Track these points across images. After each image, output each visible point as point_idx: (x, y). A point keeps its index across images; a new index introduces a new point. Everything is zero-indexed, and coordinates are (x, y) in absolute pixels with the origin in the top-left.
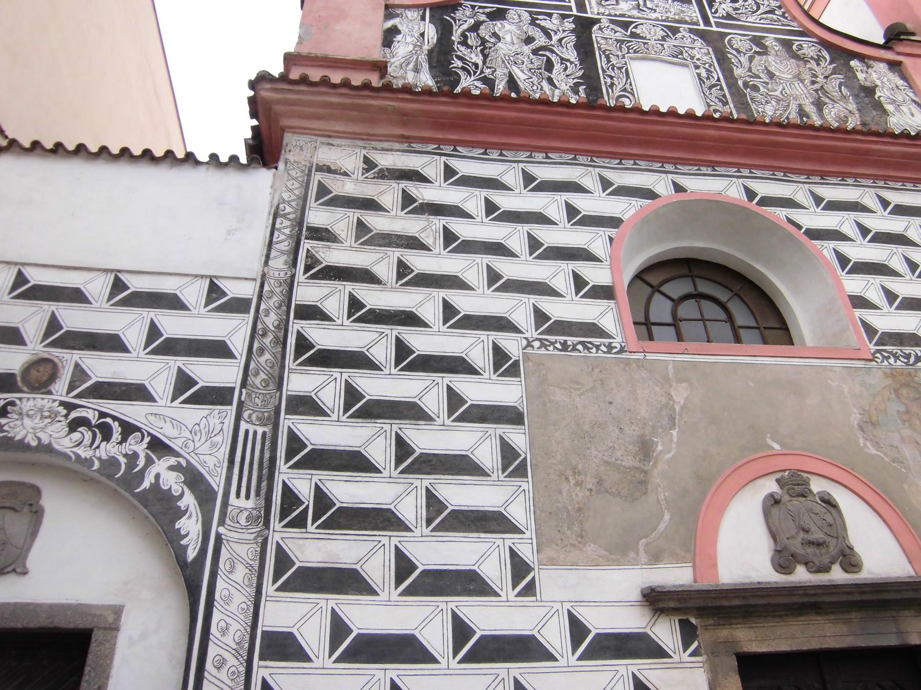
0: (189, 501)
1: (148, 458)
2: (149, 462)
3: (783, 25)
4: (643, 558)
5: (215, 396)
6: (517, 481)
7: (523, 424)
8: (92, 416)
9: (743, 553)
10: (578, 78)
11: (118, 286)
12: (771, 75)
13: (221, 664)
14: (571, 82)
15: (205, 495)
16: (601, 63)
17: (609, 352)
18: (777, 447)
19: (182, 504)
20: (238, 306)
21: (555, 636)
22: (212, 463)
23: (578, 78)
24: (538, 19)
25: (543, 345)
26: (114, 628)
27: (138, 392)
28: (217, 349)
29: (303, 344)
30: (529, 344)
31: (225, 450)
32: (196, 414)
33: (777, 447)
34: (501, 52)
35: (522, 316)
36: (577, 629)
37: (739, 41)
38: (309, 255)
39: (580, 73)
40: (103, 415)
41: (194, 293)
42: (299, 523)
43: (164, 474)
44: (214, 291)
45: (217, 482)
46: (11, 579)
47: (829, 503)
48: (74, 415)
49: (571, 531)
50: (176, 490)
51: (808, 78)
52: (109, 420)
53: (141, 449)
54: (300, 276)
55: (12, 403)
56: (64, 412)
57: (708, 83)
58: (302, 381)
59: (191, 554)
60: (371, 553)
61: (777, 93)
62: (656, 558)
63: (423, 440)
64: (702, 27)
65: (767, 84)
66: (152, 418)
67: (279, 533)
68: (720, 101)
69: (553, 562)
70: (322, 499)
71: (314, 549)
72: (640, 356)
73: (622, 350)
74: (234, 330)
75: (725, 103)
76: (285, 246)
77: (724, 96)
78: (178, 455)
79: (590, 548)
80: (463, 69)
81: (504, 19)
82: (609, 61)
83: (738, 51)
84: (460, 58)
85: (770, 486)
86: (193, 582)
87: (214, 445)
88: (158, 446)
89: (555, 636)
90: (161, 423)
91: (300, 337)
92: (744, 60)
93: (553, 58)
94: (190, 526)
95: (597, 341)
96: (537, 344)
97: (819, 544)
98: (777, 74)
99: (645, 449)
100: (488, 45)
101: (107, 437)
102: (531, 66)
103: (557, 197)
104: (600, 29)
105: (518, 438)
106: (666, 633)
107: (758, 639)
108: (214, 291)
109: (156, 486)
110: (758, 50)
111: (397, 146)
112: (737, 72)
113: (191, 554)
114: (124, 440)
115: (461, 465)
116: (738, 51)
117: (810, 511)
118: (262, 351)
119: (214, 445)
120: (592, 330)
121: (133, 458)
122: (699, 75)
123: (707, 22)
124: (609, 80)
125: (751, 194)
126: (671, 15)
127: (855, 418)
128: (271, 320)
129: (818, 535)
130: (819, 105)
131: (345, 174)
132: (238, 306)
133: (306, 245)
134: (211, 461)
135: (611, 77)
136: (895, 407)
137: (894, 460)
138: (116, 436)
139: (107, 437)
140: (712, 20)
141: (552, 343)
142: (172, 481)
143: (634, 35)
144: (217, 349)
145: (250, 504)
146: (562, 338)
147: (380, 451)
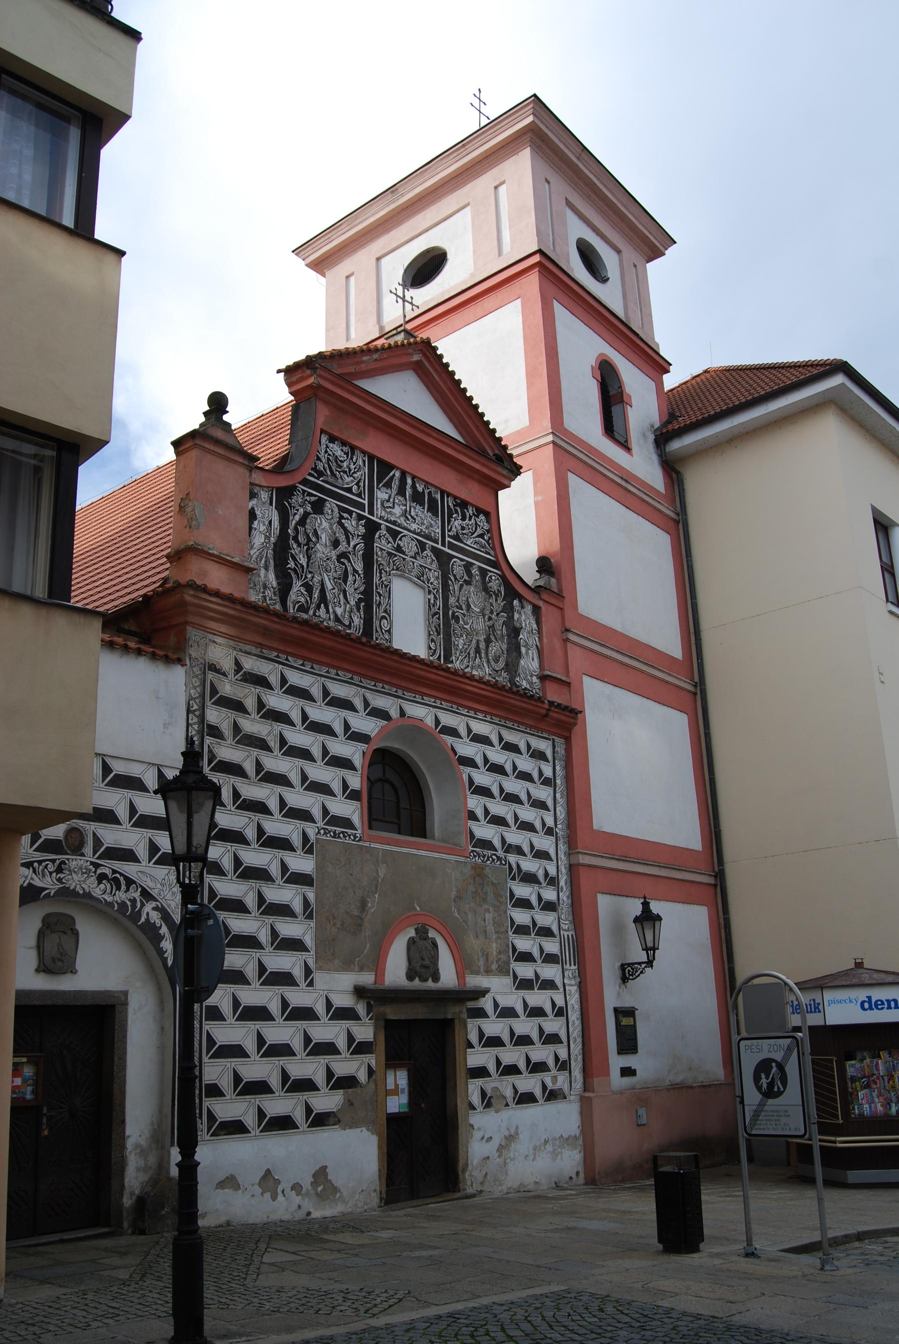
0: (164, 930)
1: (141, 901)
2: (143, 905)
6: (309, 922)
7: (313, 886)
8: (108, 871)
12: (469, 607)
16: (376, 580)
17: (354, 840)
18: (418, 909)
19: (161, 932)
21: (320, 1008)
23: (361, 593)
25: (325, 833)
27: (129, 855)
30: (319, 833)
33: (418, 909)
34: (319, 555)
36: (329, 1005)
39: (362, 589)
40: (114, 872)
46: (69, 976)
47: (435, 945)
48: (99, 871)
49: (331, 954)
50: (158, 922)
52: (117, 875)
53: (137, 895)
55: (63, 863)
56: (93, 869)
60: (248, 962)
61: (467, 627)
62: (361, 969)
64: (439, 546)
66: (140, 874)
68: (437, 630)
72: (367, 844)
75: (439, 634)
77: (439, 625)
78: (156, 900)
80: (294, 570)
81: (322, 513)
84: (294, 559)
87: (173, 893)
88: (146, 895)
89: (320, 1008)
90: (144, 879)
95: (350, 831)
96: (322, 832)
101: (119, 888)
103: (340, 713)
104: (380, 537)
106: (361, 1009)
109: (147, 920)
110: (467, 578)
111: (254, 650)
112: (452, 600)
114: (127, 890)
115: (284, 910)
116: (455, 576)
117: (426, 948)
119: (173, 893)
120: (346, 823)
121: (133, 901)
122: (429, 600)
124: (378, 598)
125: (437, 722)
126: (423, 528)
129: (427, 962)
130: (488, 641)
131: (224, 674)
134: (173, 904)
135: (380, 595)
136: (471, 888)
137: (464, 921)
138: (123, 887)
139: (119, 888)
141: (330, 832)
142: (155, 917)
143: (399, 549)
147: (250, 901)
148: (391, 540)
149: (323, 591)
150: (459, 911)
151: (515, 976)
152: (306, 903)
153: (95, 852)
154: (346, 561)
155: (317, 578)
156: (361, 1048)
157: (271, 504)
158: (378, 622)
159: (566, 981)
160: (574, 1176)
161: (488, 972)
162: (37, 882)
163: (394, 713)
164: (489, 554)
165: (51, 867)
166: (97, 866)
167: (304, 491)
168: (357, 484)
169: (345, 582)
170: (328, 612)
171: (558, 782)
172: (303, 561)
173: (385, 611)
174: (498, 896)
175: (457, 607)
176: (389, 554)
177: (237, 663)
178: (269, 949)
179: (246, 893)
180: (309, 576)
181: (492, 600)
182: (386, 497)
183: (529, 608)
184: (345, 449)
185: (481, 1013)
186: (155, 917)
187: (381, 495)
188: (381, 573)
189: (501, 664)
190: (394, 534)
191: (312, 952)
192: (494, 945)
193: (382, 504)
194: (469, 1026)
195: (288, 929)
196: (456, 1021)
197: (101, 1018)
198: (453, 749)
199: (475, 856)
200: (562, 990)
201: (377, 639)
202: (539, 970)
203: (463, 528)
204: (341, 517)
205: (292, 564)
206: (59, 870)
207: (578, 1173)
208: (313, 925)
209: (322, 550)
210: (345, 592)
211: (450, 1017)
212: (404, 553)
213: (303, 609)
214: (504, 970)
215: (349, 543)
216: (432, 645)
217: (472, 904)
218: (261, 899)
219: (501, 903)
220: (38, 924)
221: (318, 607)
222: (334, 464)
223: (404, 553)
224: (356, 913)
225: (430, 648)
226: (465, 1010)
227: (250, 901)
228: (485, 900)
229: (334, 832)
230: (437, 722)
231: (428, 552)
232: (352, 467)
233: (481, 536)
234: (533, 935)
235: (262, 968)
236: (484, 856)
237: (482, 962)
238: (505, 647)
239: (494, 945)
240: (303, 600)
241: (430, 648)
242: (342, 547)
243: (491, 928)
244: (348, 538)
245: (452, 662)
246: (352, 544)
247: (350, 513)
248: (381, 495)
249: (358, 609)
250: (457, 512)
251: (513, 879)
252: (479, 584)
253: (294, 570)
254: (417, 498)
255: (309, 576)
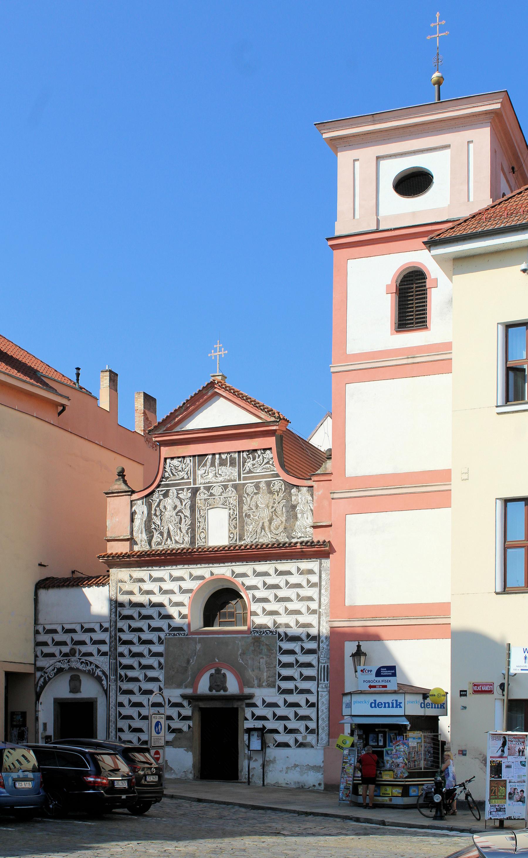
0: (103, 678)
2: (96, 670)
3: (271, 471)
4: (184, 687)
5: (105, 654)
6: (161, 670)
9: (203, 686)
10: (189, 525)
11: (82, 627)
12: (257, 506)
13: (112, 708)
14: (187, 528)
15: (106, 676)
16: (197, 515)
18: (217, 661)
20: (106, 630)
22: (106, 669)
23: (189, 525)
24: (179, 494)
25: (169, 635)
26: (97, 702)
27: (91, 654)
28: (103, 642)
29: (120, 639)
31: (108, 666)
32: (102, 658)
33: (217, 661)
35: (165, 627)
37: (250, 489)
38: (120, 613)
40: (86, 660)
41: (97, 628)
42: (122, 681)
43: (98, 672)
44: (101, 626)
45: (108, 673)
47: (224, 675)
49: (170, 681)
51: (271, 504)
53: (94, 667)
54: (118, 620)
57: (232, 517)
58: (121, 649)
59: (105, 688)
60: (134, 687)
61: (256, 518)
62: (186, 687)
63: (144, 662)
64: (237, 482)
65: (254, 512)
67: (119, 683)
69: (167, 688)
70: (126, 676)
71: (126, 686)
72: (190, 636)
73: (187, 635)
74: (105, 636)
76: (114, 610)
77: (236, 524)
79: (174, 685)
80: (155, 529)
82: (200, 513)
83: (248, 494)
85: (213, 671)
86: (106, 692)
88: (97, 667)
91: (119, 637)
92: (249, 499)
93: (183, 516)
94: (104, 682)
97: (218, 686)
98: (260, 505)
99: (188, 661)
100: (163, 513)
102: (175, 522)
105: (162, 660)
106: (185, 703)
107: (202, 705)
108: (101, 626)
109: (98, 675)
110: (256, 491)
112: (245, 508)
113: (105, 688)
115: (151, 667)
116: (248, 494)
118: (112, 642)
123: (240, 479)
126: (227, 477)
127: (240, 652)
128: (113, 633)
129: (219, 683)
130: (271, 521)
132: (106, 630)
133: (119, 609)
134: (106, 669)
135: (200, 522)
136: (252, 648)
139: (88, 665)
140: (242, 476)
142: (100, 674)
143: (212, 495)
144: (103, 642)
145: (114, 677)
146: (173, 632)
147: (136, 665)
148: (206, 492)
149: (169, 532)
150: (242, 660)
151: (279, 688)
152: (160, 664)
153: (79, 655)
154: (180, 514)
155: (166, 527)
156: (186, 718)
157: (143, 504)
158: (198, 536)
159: (319, 689)
160: (317, 785)
161: (260, 686)
162: (62, 666)
163: (207, 576)
164: (273, 471)
165: (66, 661)
166: (80, 659)
167: (159, 491)
168: (187, 474)
169: (180, 524)
170: (171, 540)
171: (323, 583)
172: (158, 523)
173: (203, 529)
174: (270, 650)
175: (249, 510)
176: (205, 500)
177: (131, 576)
178: (143, 682)
179: (134, 662)
180: (162, 528)
181: (275, 496)
182: (204, 472)
183: (304, 489)
184: (180, 459)
185: (254, 705)
186: (100, 674)
187: (200, 472)
188: (200, 512)
189: (281, 529)
190: (208, 489)
191: (163, 682)
192: (265, 674)
193: (202, 477)
194: (246, 711)
195: (151, 674)
196: (239, 709)
197: (89, 706)
198: (242, 583)
199: (254, 633)
200: (316, 694)
201: (198, 544)
202: (298, 685)
203: (253, 465)
204: (178, 494)
205: (153, 526)
206: (69, 662)
207: (320, 784)
208: (163, 671)
209: (169, 513)
210: (180, 528)
211: (235, 706)
212: (214, 495)
213: (159, 544)
214: (272, 685)
215: (182, 505)
216: (232, 536)
217: (252, 656)
218: (140, 664)
219: (272, 653)
220: (69, 678)
221: (167, 540)
222: (174, 470)
223: (214, 495)
224: (185, 665)
225: (230, 537)
226: (244, 704)
227: (136, 665)
228: (260, 653)
229: (174, 634)
230: (233, 572)
231: (230, 488)
232: (184, 466)
233: (268, 463)
234: (295, 667)
235: (140, 689)
236: (261, 632)
237: (256, 682)
238: (284, 519)
239: (265, 674)
240: (159, 540)
241: (230, 537)
242: (178, 509)
243: (263, 666)
244: (181, 502)
245: (245, 540)
246: (184, 504)
247: (183, 490)
248: (200, 472)
249: (188, 534)
250: (249, 458)
251: (282, 640)
252: (266, 491)
253: (155, 529)
254: (223, 463)
255: (162, 528)
